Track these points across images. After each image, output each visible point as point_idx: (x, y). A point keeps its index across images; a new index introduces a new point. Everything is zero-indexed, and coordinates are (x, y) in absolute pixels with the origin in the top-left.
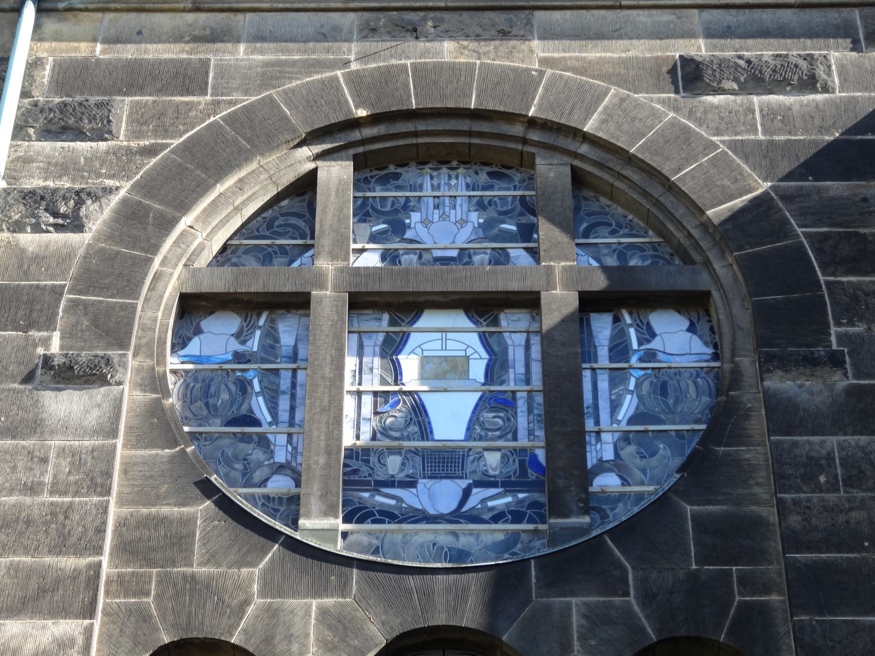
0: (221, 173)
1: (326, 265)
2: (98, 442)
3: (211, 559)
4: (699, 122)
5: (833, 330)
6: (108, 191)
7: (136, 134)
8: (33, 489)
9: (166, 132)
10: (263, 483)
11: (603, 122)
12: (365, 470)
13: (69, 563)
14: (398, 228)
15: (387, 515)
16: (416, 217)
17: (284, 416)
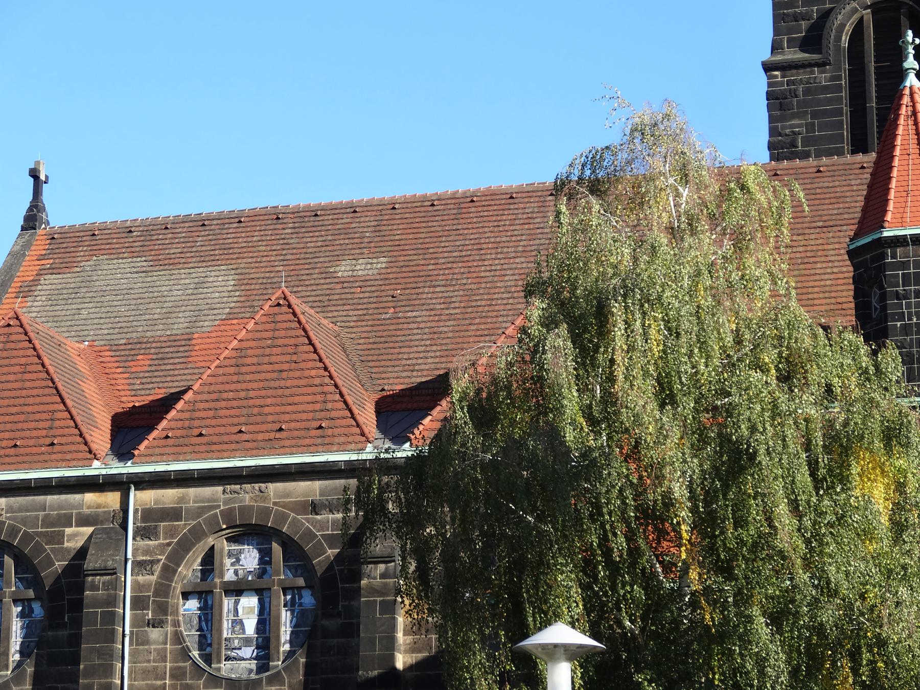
0: (187, 552)
1: (217, 580)
2: (163, 646)
3: (191, 679)
4: (314, 527)
5: (340, 604)
6: (159, 561)
7: (165, 538)
8: (149, 661)
9: (172, 536)
10: (205, 650)
11: (288, 527)
12: (229, 645)
13: (159, 683)
14: (238, 560)
15: (235, 659)
16: (243, 555)
17: (210, 628)
